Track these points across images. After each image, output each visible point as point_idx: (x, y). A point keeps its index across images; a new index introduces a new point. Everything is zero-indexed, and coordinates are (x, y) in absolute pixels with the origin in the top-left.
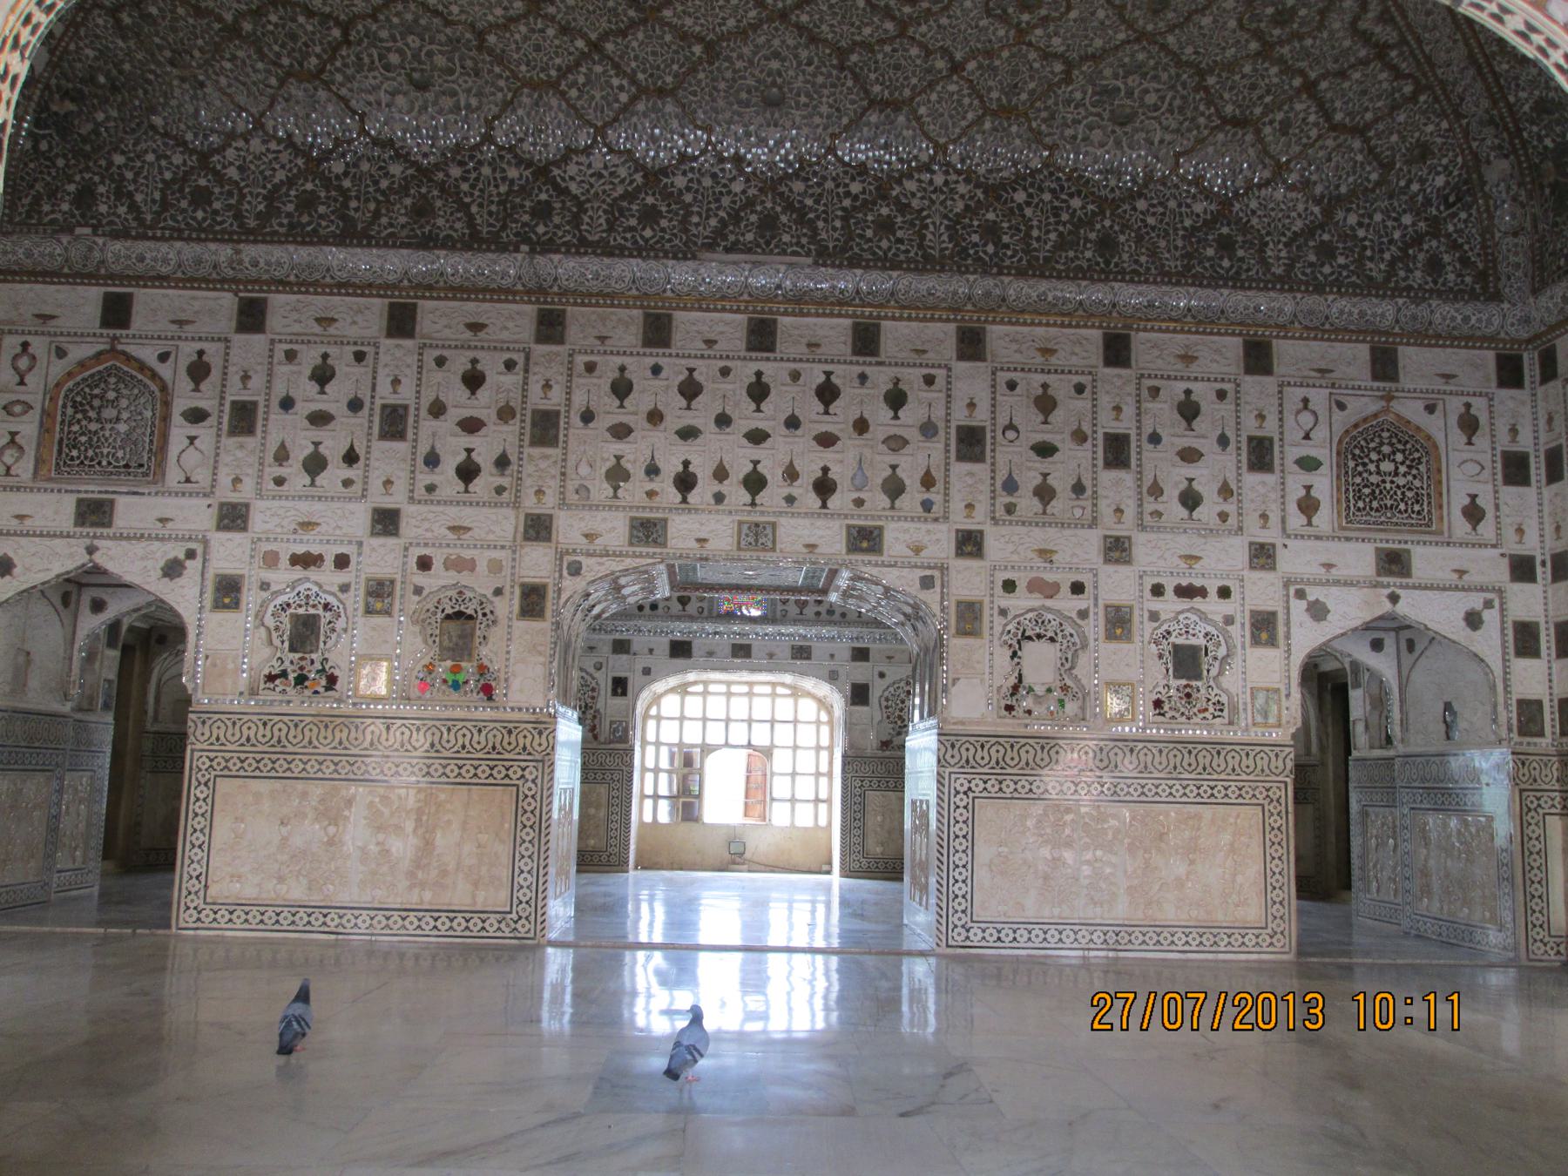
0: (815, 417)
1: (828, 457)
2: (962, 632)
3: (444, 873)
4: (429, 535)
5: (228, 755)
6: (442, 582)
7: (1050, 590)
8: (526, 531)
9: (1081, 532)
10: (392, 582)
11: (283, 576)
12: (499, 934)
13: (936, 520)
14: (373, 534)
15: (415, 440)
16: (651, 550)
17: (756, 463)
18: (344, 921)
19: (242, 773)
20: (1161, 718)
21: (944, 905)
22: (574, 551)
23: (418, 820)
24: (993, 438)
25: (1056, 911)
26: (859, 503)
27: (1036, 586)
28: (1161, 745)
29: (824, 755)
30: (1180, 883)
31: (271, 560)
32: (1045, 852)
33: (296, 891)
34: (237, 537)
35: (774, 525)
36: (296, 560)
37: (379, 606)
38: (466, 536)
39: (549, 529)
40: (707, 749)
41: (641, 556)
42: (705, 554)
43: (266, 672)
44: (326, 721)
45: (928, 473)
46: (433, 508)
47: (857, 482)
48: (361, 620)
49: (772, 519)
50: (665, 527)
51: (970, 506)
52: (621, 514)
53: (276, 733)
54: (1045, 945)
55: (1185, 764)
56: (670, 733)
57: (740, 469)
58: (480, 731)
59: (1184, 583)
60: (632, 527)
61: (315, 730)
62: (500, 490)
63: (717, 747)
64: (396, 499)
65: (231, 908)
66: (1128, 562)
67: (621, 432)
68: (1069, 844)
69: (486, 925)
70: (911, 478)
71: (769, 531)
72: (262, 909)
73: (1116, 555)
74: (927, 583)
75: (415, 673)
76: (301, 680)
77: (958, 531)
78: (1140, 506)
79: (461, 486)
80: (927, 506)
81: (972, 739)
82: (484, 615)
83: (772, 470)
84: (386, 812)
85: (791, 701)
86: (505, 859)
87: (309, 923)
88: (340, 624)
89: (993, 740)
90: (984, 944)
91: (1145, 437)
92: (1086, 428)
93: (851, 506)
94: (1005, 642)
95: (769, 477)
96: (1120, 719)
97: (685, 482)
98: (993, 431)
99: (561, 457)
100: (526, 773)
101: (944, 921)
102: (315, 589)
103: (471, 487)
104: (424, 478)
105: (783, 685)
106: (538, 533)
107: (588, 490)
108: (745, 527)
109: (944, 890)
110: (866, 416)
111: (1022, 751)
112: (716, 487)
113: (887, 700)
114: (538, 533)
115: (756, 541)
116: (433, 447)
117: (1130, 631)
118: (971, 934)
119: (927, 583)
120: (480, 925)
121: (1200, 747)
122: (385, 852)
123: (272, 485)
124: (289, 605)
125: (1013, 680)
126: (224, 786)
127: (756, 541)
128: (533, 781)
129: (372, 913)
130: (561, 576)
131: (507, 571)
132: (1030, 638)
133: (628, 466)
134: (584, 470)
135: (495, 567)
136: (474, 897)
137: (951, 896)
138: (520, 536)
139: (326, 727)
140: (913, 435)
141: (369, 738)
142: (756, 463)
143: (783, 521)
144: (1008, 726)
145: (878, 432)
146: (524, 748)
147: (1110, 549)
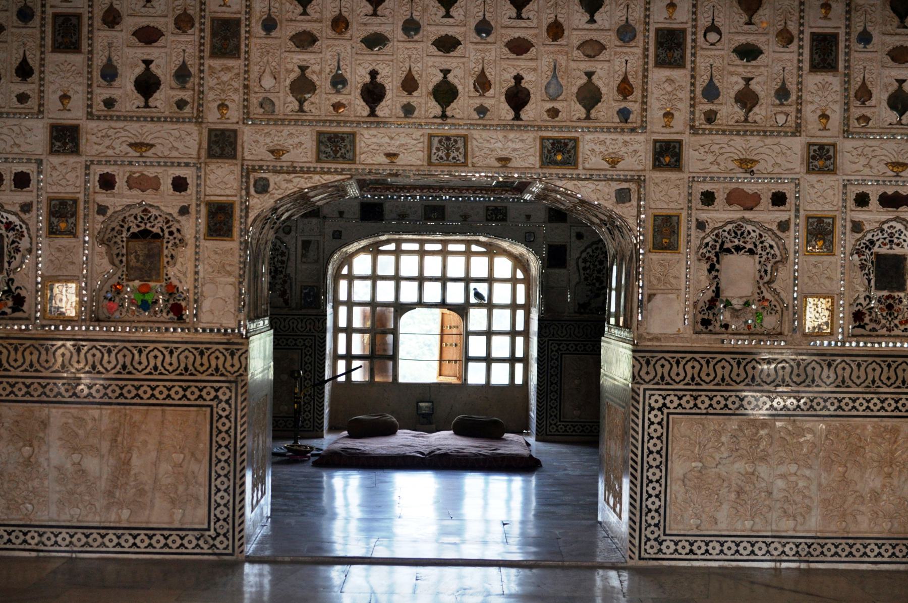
0: (508, 22)
1: (521, 65)
2: (659, 247)
4: (110, 152)
6: (126, 201)
7: (749, 201)
8: (209, 147)
9: (784, 141)
10: (75, 201)
12: (197, 550)
13: (633, 130)
14: (53, 152)
15: (91, 52)
16: (340, 166)
17: (446, 72)
18: (44, 539)
20: (860, 331)
21: (637, 519)
22: (261, 167)
24: (694, 41)
25: (748, 524)
26: (554, 113)
27: (737, 198)
28: (859, 359)
29: (520, 314)
30: (876, 496)
32: (741, 466)
35: (465, 138)
37: (63, 225)
38: (149, 153)
39: (233, 144)
40: (401, 308)
41: (329, 172)
42: (395, 169)
44: (17, 342)
45: (625, 80)
46: (113, 124)
47: (552, 91)
48: (43, 242)
49: (463, 132)
50: (353, 143)
51: (668, 115)
52: (308, 129)
54: (738, 557)
55: (884, 378)
56: (362, 291)
57: (430, 79)
58: (171, 353)
59: (890, 191)
60: (319, 142)
62: (181, 104)
63: (409, 307)
64: (75, 115)
66: (832, 171)
67: (305, 40)
68: (763, 459)
69: (185, 542)
70: (606, 83)
71: (460, 144)
73: (819, 163)
74: (622, 196)
75: (103, 293)
77: (655, 141)
78: (847, 110)
79: (140, 101)
80: (624, 114)
81: (667, 356)
82: (171, 233)
83: (463, 81)
84: (81, 432)
85: (485, 260)
86: (203, 479)
88: (24, 243)
89: (689, 356)
90: (677, 556)
91: (854, 36)
92: (793, 28)
93: (545, 116)
94: (703, 255)
95: (460, 88)
96: (818, 334)
97: (373, 93)
98: (694, 33)
99: (243, 68)
100: (220, 394)
101: (637, 535)
103: (152, 102)
104: (102, 93)
105: (478, 243)
106: (223, 149)
107: (273, 104)
108: (435, 141)
109: (638, 505)
110: (561, 20)
111: (718, 367)
112: (405, 99)
113: (585, 261)
114: (223, 149)
115: (448, 155)
116: (109, 59)
117: (832, 242)
118: (663, 547)
119: (622, 196)
120: (179, 542)
121: (900, 360)
125: (710, 294)
127: (448, 155)
128: (227, 402)
129: (72, 531)
130: (248, 194)
131: (192, 189)
132: (728, 251)
133: (314, 78)
134: (268, 82)
135: (180, 185)
136: (171, 515)
137: (645, 510)
138: (203, 153)
139: (16, 349)
140: (610, 39)
141: (60, 360)
142: (446, 72)
143: (476, 134)
144: (706, 342)
145: (573, 38)
146: (217, 369)
147: (814, 158)
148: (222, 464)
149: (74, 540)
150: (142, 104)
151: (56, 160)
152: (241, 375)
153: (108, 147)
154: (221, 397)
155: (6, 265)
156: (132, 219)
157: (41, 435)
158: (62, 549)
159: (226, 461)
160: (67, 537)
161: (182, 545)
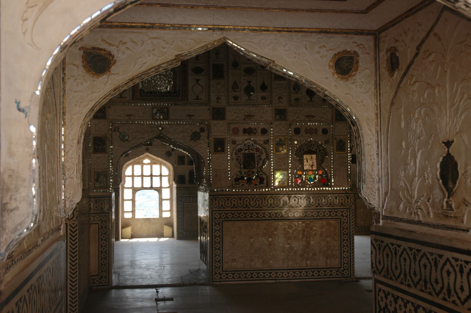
3: (314, 254)
5: (227, 212)
11: (240, 138)
12: (337, 276)
14: (276, 120)
19: (233, 219)
23: (303, 234)
31: (236, 132)
33: (258, 265)
34: (221, 122)
36: (245, 131)
43: (235, 177)
53: (245, 203)
61: (260, 200)
65: (233, 273)
72: (246, 272)
76: (250, 180)
79: (309, 99)
87: (264, 276)
88: (264, 156)
100: (343, 213)
102: (252, 142)
122: (291, 248)
123: (232, 100)
124: (241, 149)
126: (226, 224)
128: (346, 216)
129: (288, 271)
136: (326, 262)
141: (282, 203)
148: (345, 241)
149: (290, 274)
150: (309, 100)
151: (276, 123)
152: (351, 206)
153: (297, 117)
154: (344, 215)
155: (256, 166)
156: (304, 145)
157: (276, 233)
158: (285, 278)
159: (347, 240)
160: (287, 273)
161: (331, 274)
